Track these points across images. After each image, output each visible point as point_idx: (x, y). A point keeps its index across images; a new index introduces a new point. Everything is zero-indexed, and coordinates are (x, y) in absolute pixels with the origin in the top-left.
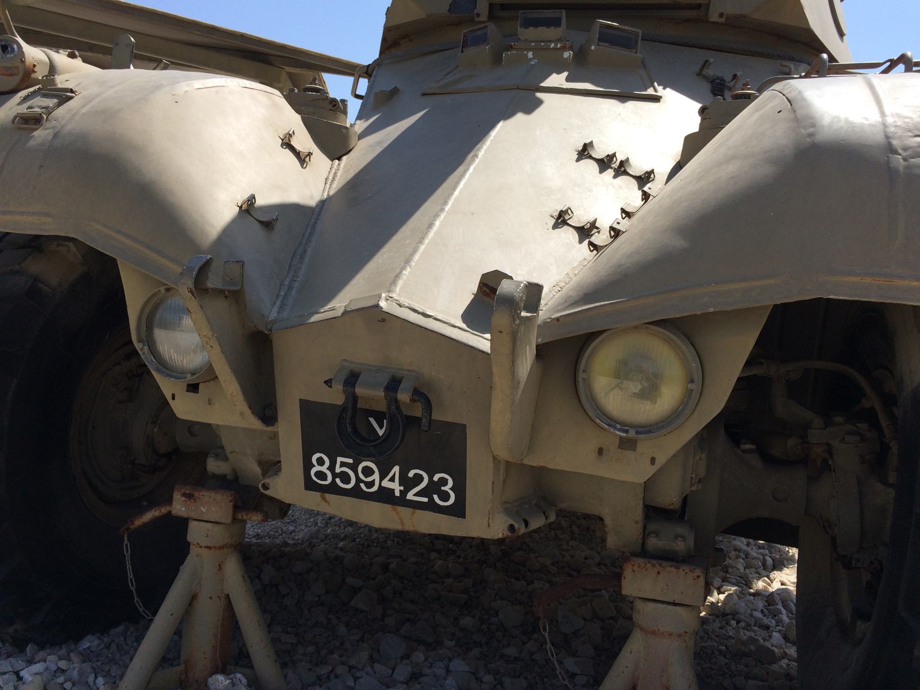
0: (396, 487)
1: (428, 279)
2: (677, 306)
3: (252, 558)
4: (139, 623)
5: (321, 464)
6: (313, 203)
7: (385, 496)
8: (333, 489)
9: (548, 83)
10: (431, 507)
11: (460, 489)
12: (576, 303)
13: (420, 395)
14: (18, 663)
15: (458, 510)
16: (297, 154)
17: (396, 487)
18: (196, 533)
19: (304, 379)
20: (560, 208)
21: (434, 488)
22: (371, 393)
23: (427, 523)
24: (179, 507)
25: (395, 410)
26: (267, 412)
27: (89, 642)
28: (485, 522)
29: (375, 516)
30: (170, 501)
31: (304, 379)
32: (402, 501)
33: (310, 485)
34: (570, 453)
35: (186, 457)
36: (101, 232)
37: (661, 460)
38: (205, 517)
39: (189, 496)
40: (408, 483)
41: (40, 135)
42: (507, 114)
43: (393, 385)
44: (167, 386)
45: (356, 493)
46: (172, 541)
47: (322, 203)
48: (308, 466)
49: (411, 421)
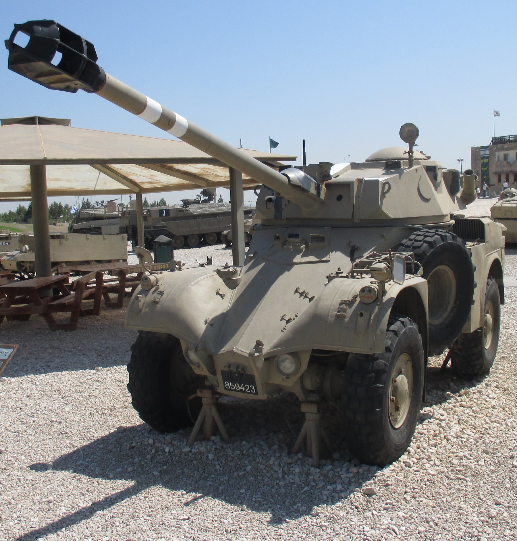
0: (243, 388)
1: (242, 344)
2: (294, 349)
3: (221, 408)
4: (192, 425)
5: (227, 384)
6: (225, 311)
7: (241, 391)
8: (230, 389)
9: (295, 260)
10: (251, 393)
11: (256, 388)
12: (275, 347)
13: (243, 369)
14: (164, 436)
15: (256, 393)
16: (221, 295)
17: (243, 388)
18: (204, 401)
19: (220, 366)
20: (283, 314)
21: (251, 389)
22: (233, 369)
23: (251, 397)
24: (199, 394)
25: (239, 373)
26: (214, 373)
27: (180, 431)
28: (262, 396)
29: (240, 395)
30: (196, 392)
31: (220, 366)
32: (245, 392)
33: (226, 389)
34: (277, 380)
35: (199, 381)
36: (175, 332)
37: (294, 381)
38: (206, 396)
39: (201, 391)
40: (246, 388)
41: (159, 306)
42: (281, 273)
43: (238, 367)
44: (193, 367)
45: (235, 390)
46: (198, 404)
47: (227, 312)
48: (224, 385)
49: (242, 374)
